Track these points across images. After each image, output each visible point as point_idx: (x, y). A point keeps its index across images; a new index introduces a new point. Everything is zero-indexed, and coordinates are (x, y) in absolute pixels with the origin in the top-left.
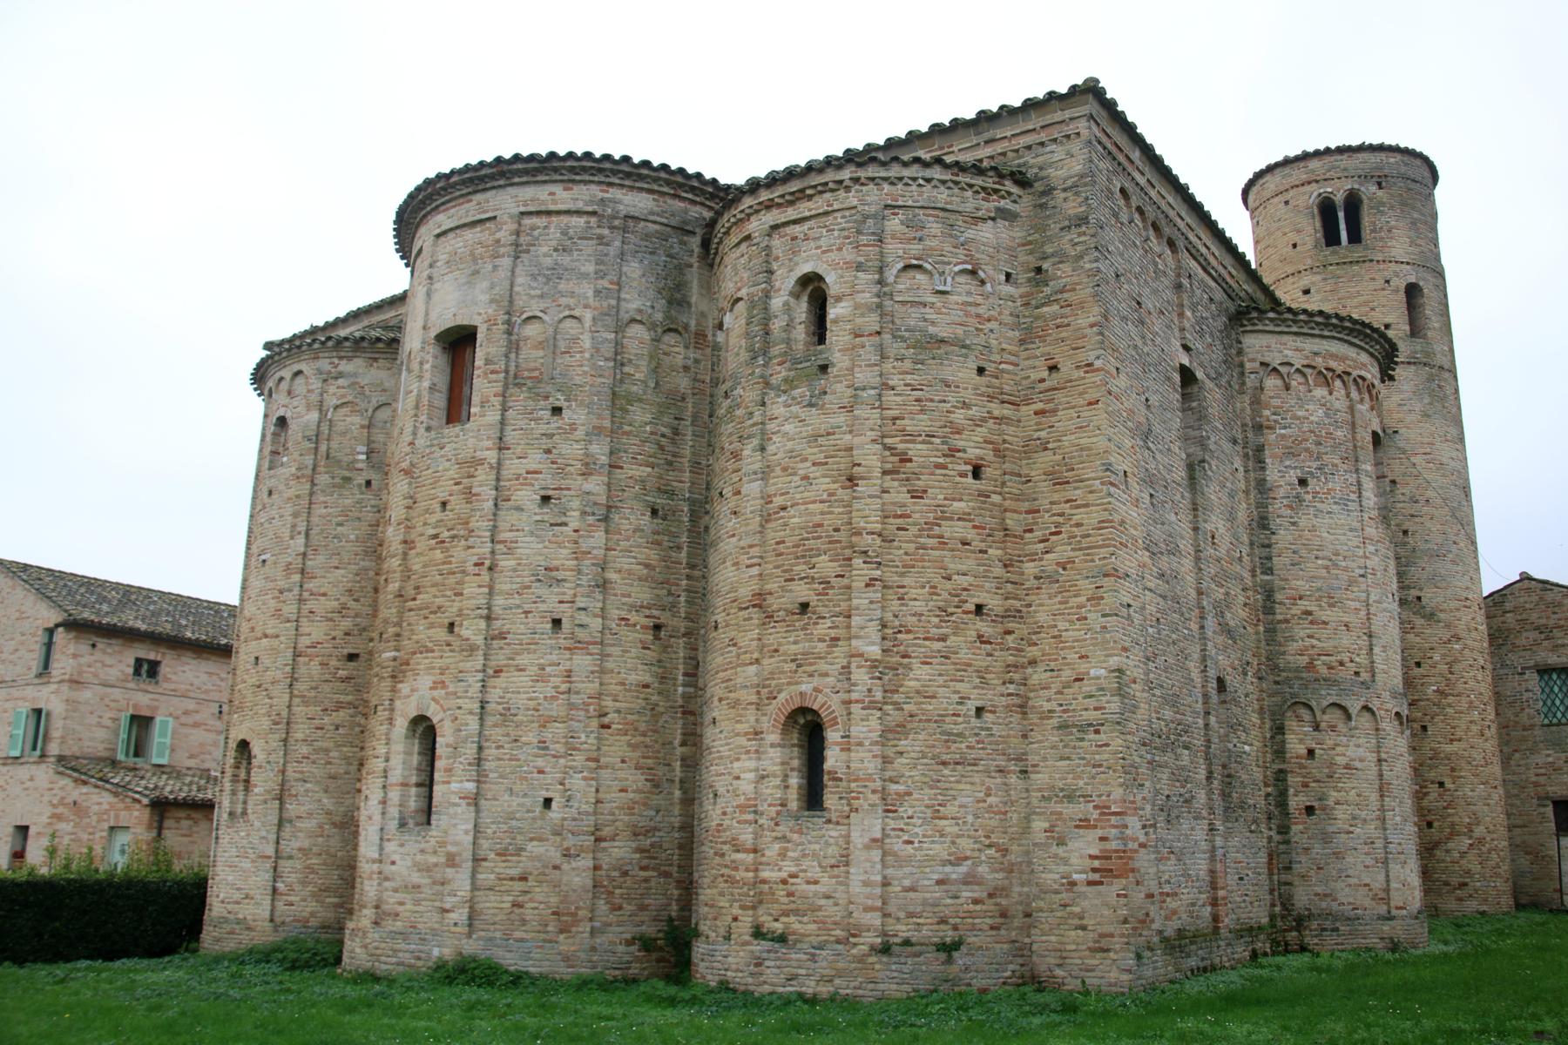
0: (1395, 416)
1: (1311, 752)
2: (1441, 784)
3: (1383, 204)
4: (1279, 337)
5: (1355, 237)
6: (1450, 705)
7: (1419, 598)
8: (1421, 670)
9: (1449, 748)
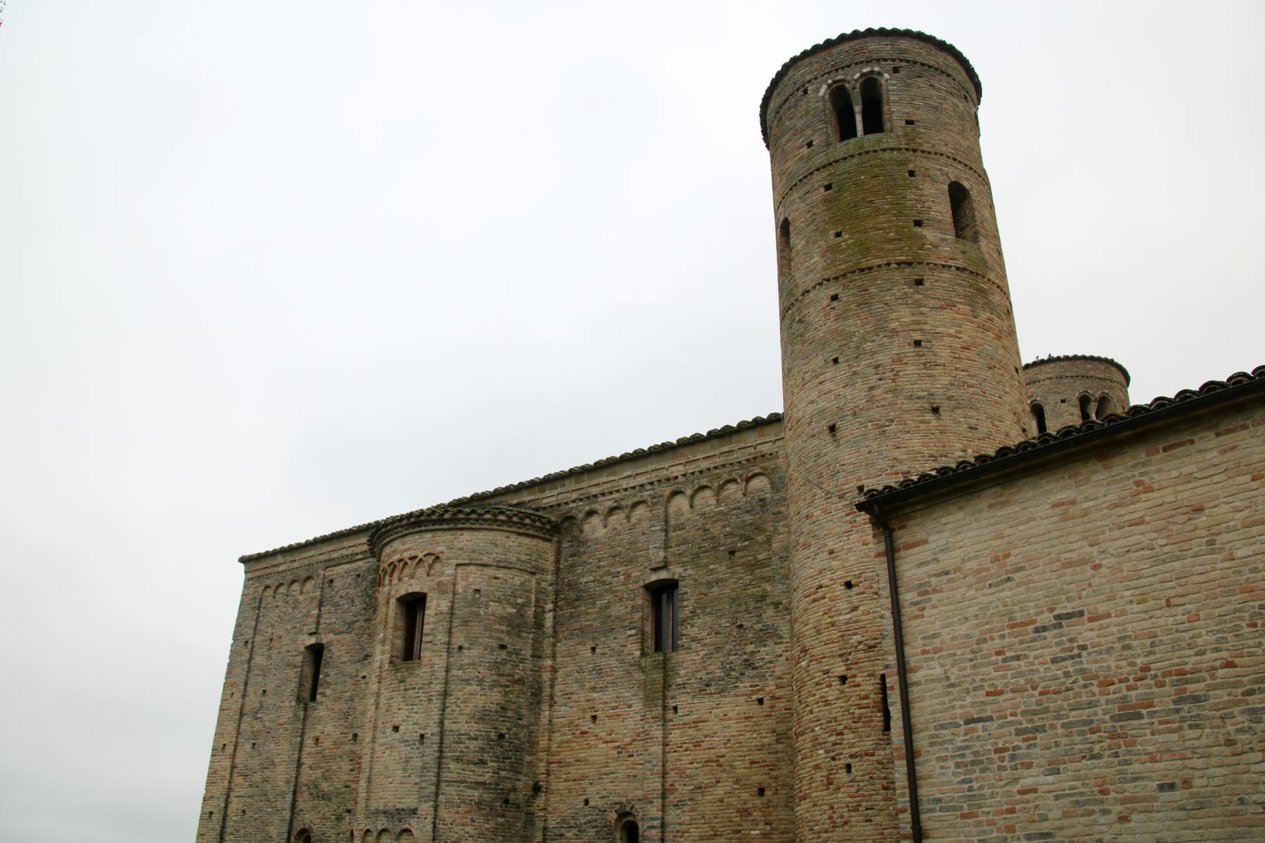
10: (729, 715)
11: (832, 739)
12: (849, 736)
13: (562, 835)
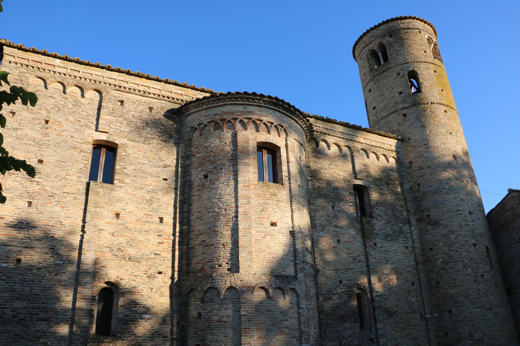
0: (408, 131)
1: (200, 314)
2: (450, 312)
3: (393, 43)
4: (199, 113)
5: (386, 59)
6: (450, 268)
7: (429, 216)
8: (433, 252)
9: (452, 291)
10: (398, 251)
11: (475, 265)
12: (481, 266)
13: (330, 298)
